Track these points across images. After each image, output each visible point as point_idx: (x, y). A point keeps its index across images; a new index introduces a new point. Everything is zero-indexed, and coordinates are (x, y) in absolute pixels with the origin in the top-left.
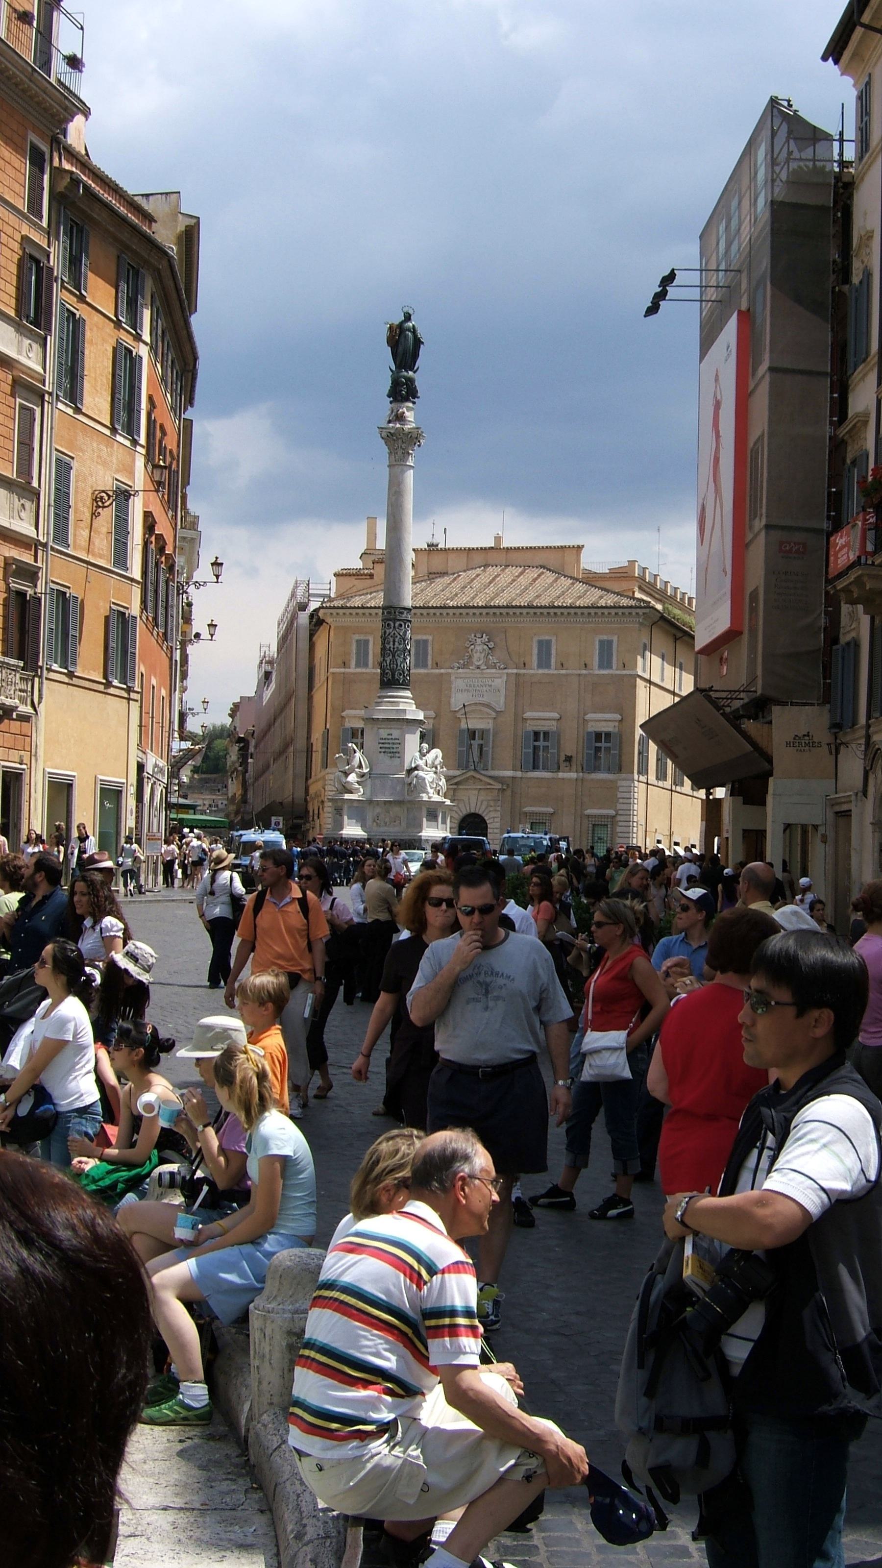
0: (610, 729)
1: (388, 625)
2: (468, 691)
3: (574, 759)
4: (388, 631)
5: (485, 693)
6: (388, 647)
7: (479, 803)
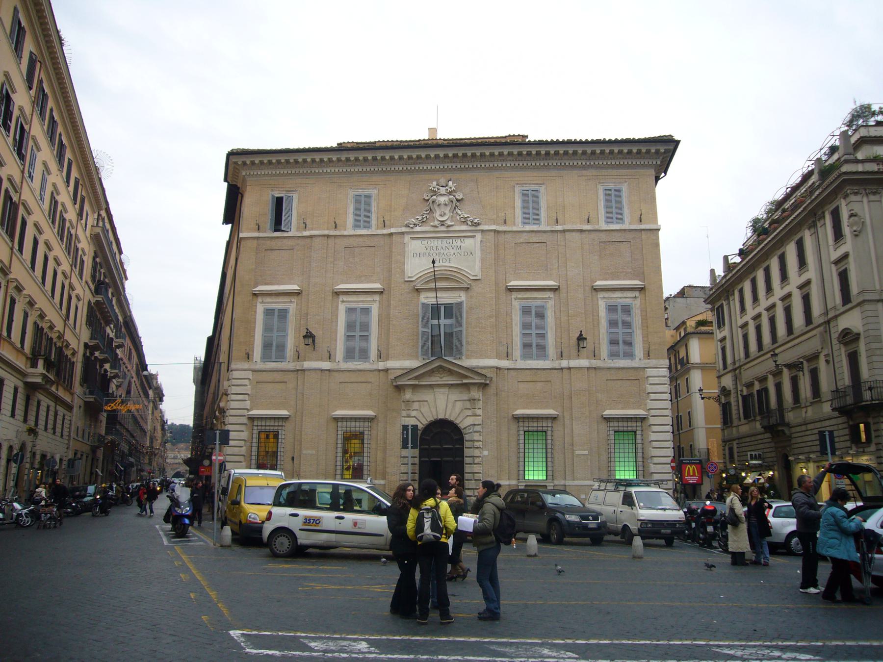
5: (452, 257)
7: (450, 405)
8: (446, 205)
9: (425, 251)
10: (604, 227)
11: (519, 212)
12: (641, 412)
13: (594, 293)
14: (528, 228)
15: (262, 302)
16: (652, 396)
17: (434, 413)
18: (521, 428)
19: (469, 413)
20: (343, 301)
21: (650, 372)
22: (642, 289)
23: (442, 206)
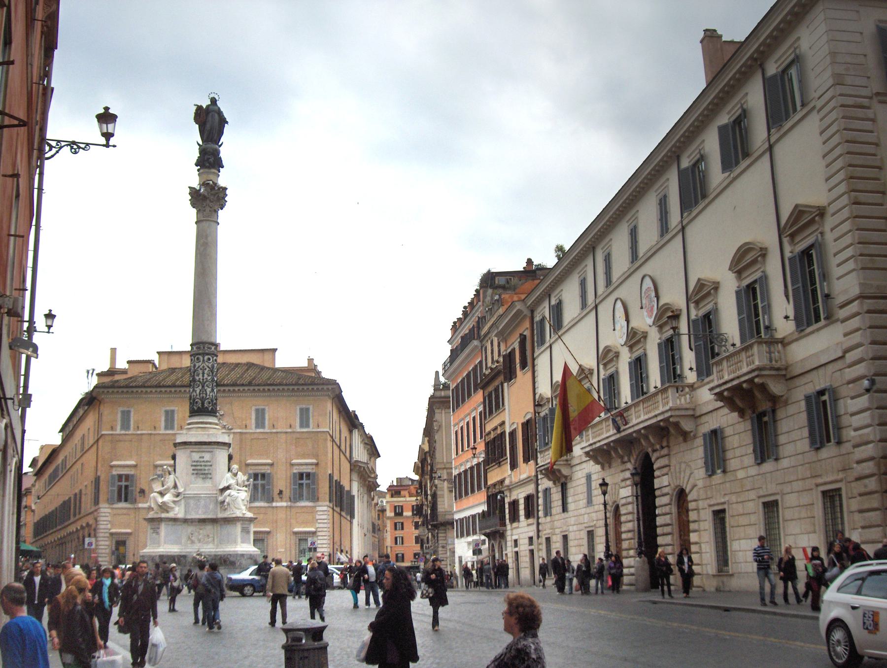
0: (309, 471)
1: (198, 359)
3: (284, 493)
4: (197, 365)
6: (197, 378)
10: (298, 430)
11: (253, 421)
12: (313, 529)
14: (258, 431)
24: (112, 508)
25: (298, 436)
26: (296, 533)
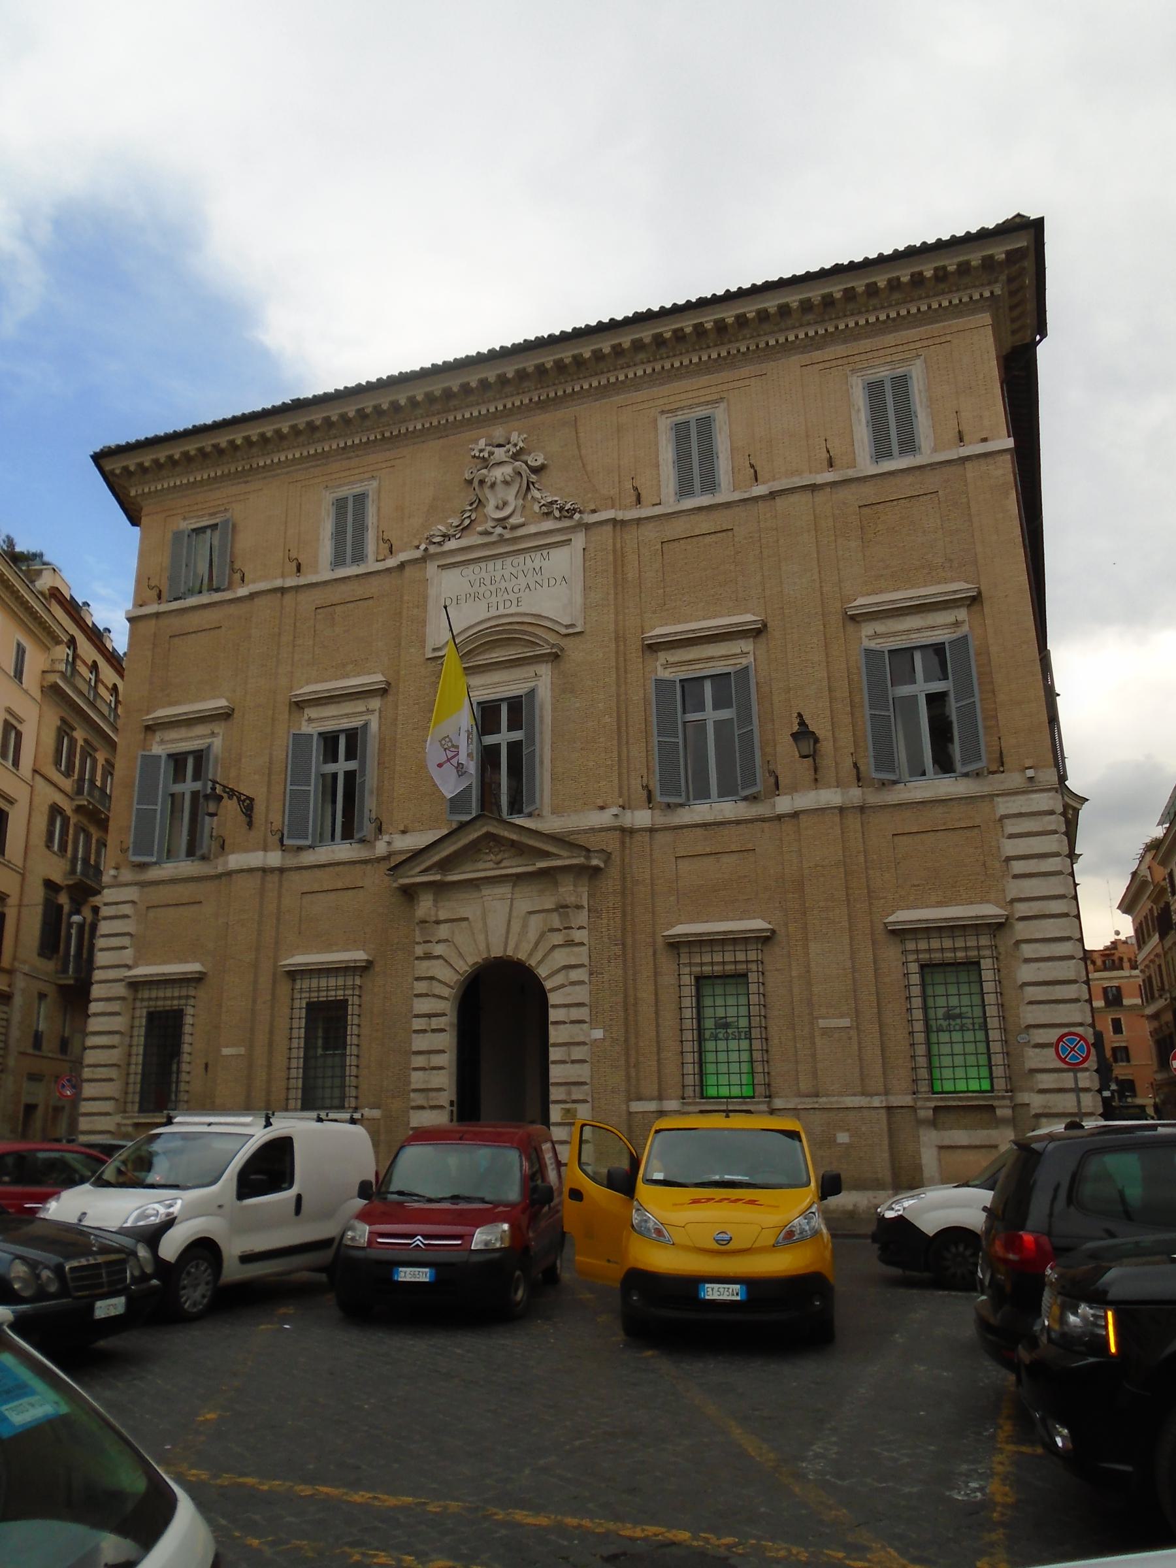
2: (476, 597)
7: (516, 927)
8: (506, 483)
9: (471, 591)
10: (867, 467)
12: (990, 910)
13: (851, 627)
14: (689, 503)
15: (162, 742)
16: (1018, 867)
17: (482, 947)
18: (686, 970)
19: (558, 939)
20: (310, 720)
21: (1005, 806)
22: (974, 601)
23: (500, 488)
24: (142, 885)
25: (868, 493)
26: (900, 934)
